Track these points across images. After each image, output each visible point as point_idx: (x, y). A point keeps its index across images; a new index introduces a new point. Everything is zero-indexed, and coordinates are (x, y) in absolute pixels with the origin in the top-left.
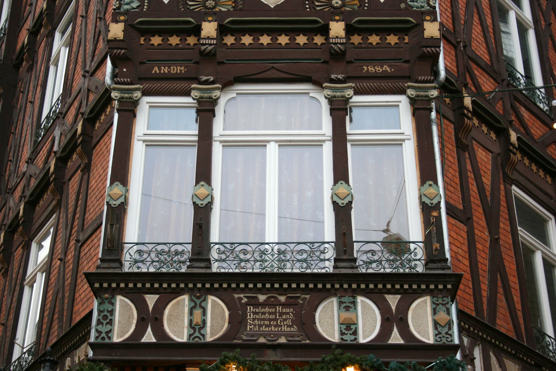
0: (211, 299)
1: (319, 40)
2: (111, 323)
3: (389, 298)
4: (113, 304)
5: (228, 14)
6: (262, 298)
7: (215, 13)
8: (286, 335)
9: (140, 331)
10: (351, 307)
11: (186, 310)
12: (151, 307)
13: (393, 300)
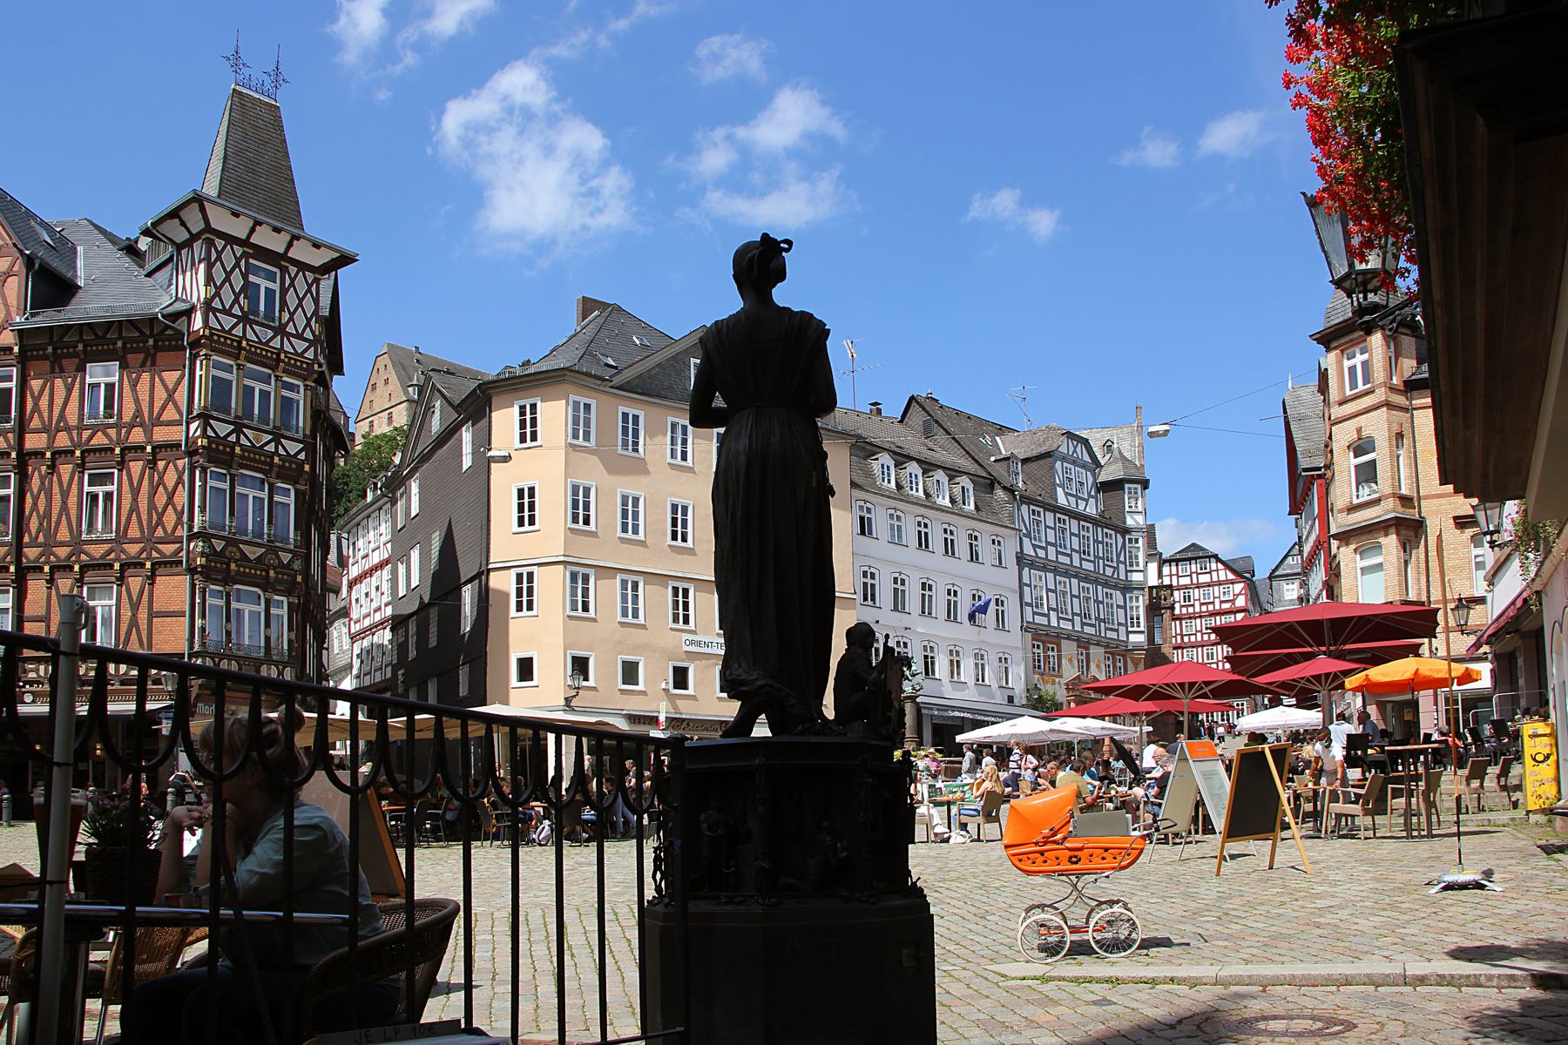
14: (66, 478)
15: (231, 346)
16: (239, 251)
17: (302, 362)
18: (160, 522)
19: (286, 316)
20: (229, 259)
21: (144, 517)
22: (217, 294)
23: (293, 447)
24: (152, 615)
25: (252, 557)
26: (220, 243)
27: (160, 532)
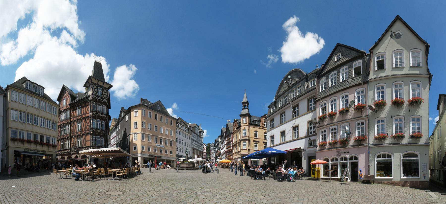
14: (75, 124)
16: (96, 85)
18: (87, 128)
21: (85, 127)
23: (104, 116)
24: (86, 141)
27: (87, 129)
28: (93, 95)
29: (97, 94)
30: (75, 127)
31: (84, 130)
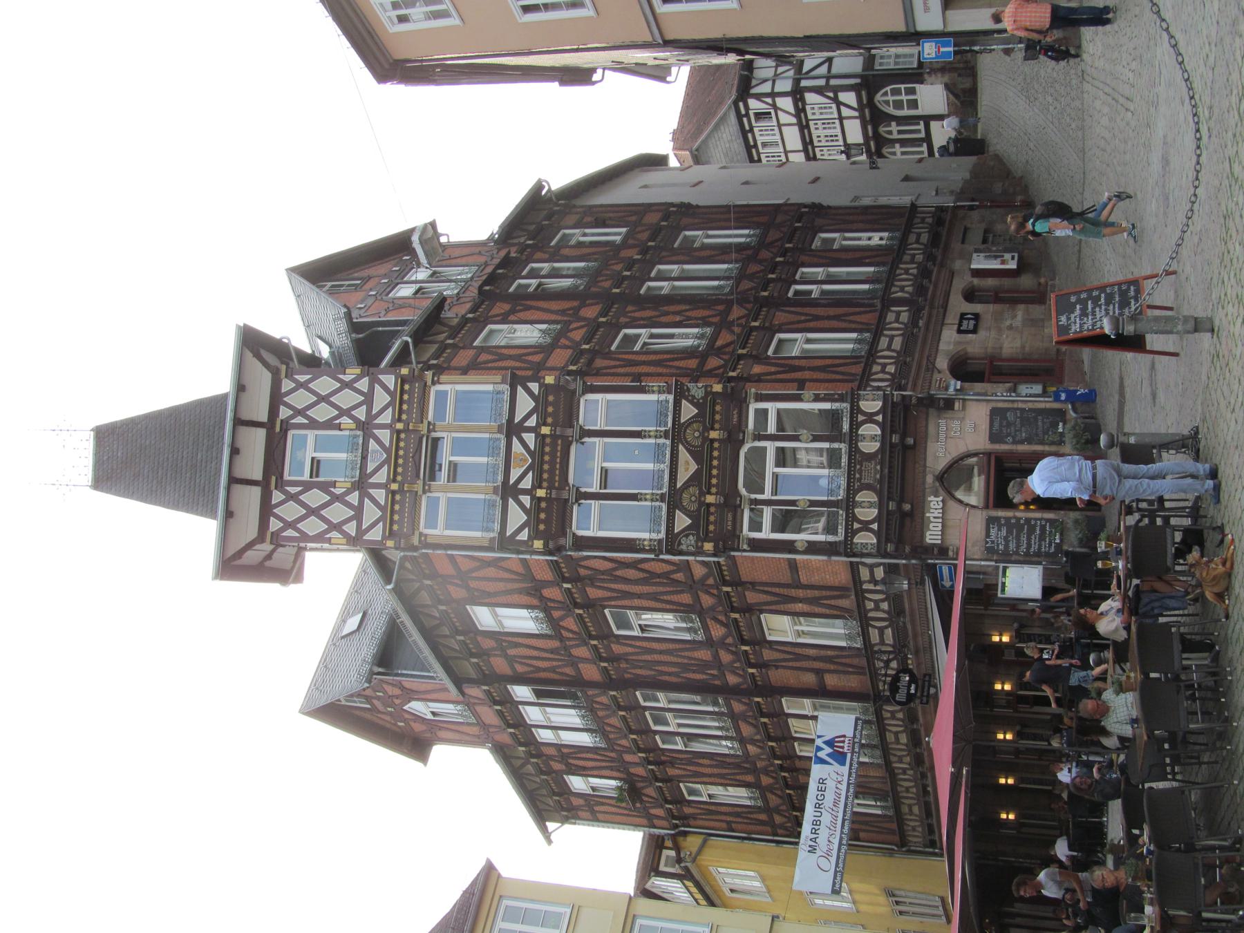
0: (857, 499)
1: (716, 445)
2: (867, 544)
3: (859, 420)
4: (858, 543)
5: (700, 489)
6: (857, 476)
7: (700, 496)
8: (876, 465)
9: (871, 531)
10: (864, 438)
11: (862, 510)
12: (860, 526)
13: (861, 418)
15: (411, 392)
16: (277, 496)
17: (398, 448)
18: (666, 575)
19: (345, 421)
20: (290, 511)
21: (661, 589)
22: (337, 527)
23: (525, 404)
24: (798, 585)
25: (694, 466)
26: (274, 525)
27: (679, 576)
28: (361, 532)
29: (348, 492)
30: (661, 652)
31: (686, 598)
